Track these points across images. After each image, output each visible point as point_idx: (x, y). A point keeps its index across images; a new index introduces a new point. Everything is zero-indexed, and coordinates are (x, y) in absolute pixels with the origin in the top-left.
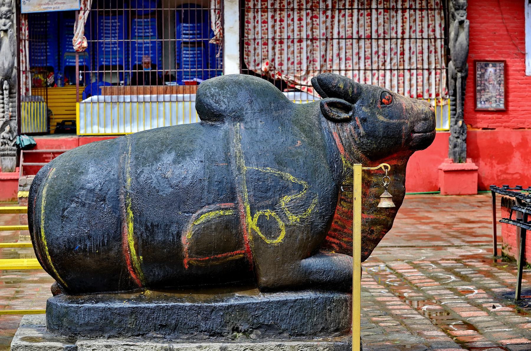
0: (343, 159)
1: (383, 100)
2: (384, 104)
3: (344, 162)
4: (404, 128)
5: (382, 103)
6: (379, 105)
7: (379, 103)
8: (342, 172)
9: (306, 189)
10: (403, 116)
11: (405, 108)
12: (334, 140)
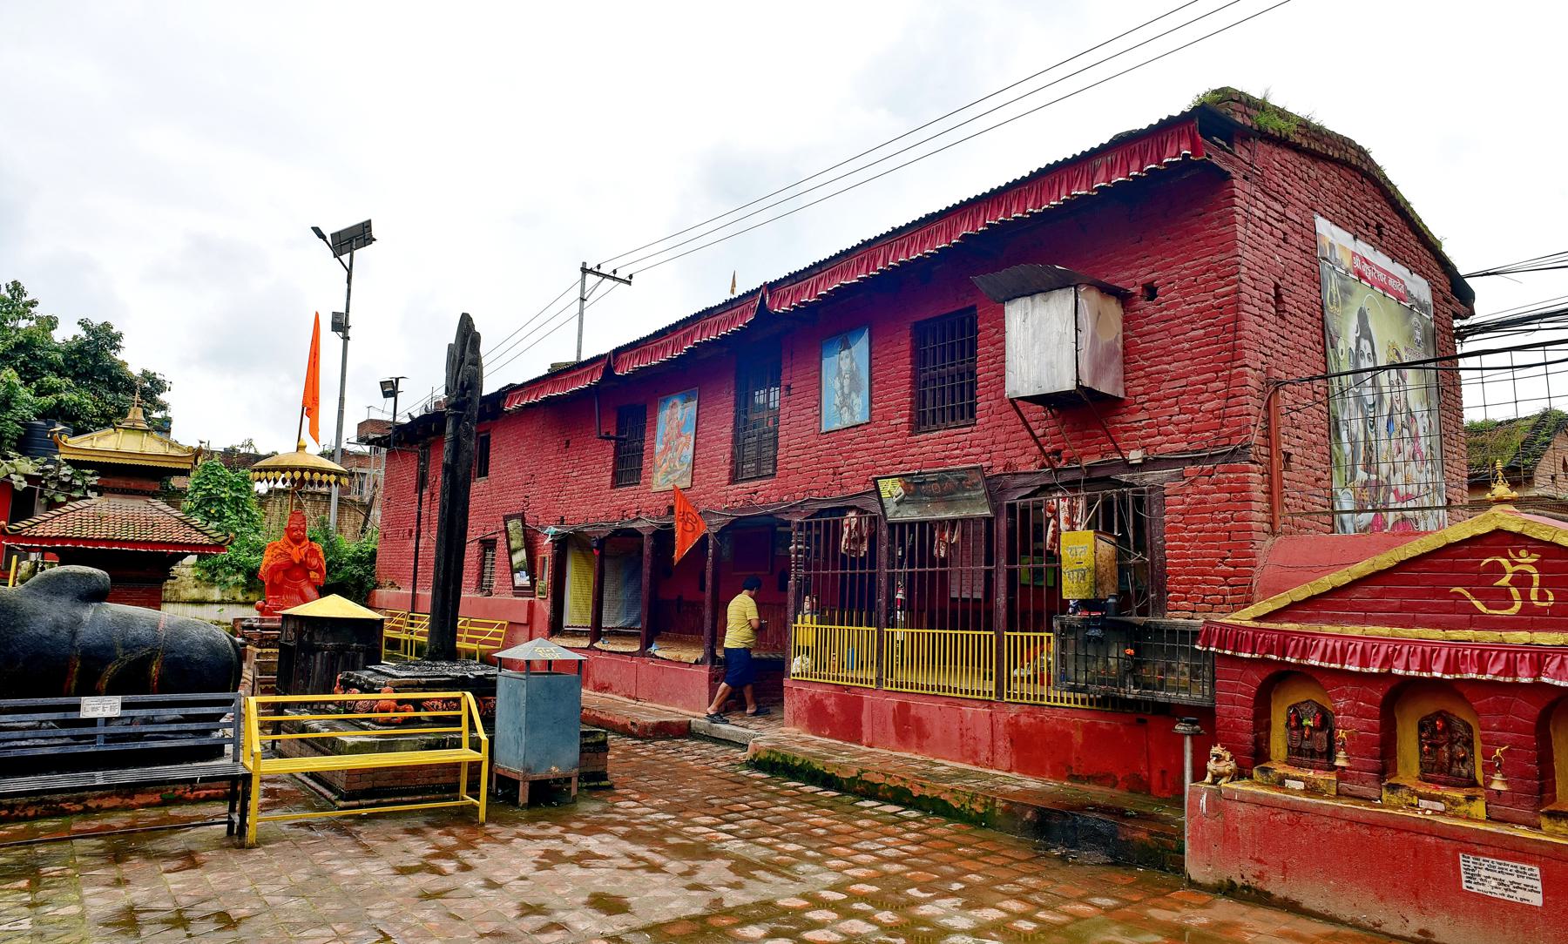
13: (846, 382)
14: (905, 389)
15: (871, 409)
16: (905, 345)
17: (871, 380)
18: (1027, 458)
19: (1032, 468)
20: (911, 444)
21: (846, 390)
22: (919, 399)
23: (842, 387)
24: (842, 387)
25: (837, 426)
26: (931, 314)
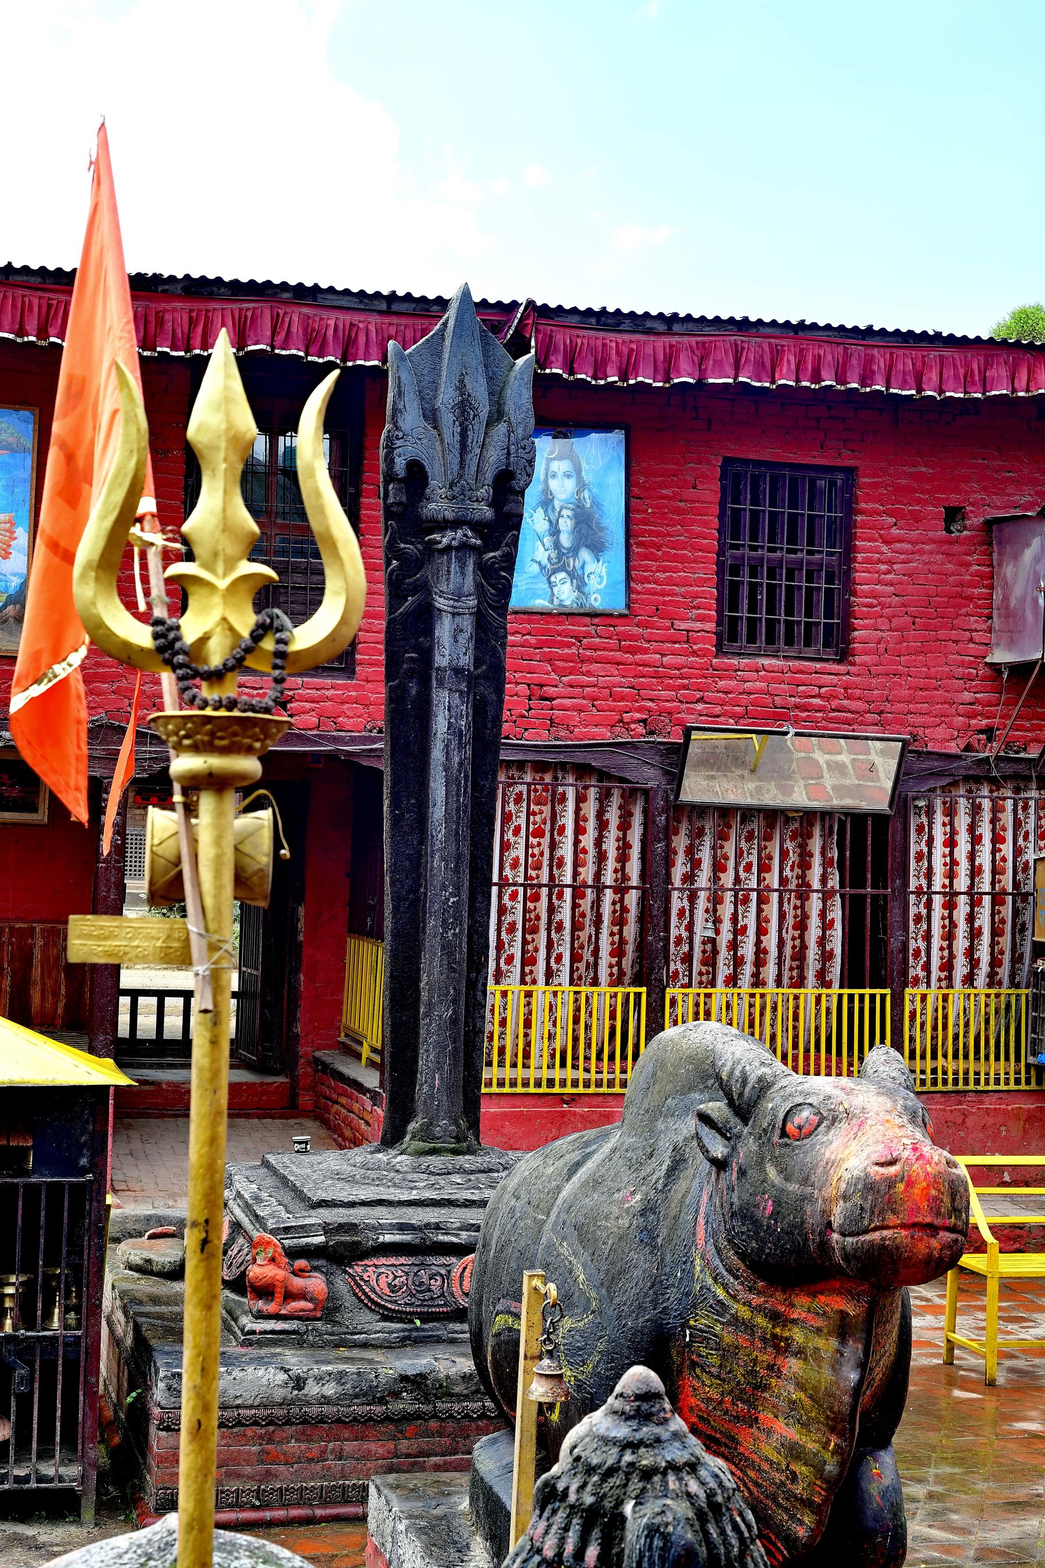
0: (698, 1261)
1: (790, 1127)
2: (788, 1137)
3: (698, 1268)
4: (808, 1209)
5: (784, 1134)
6: (776, 1138)
7: (778, 1132)
8: (688, 1294)
9: (593, 1312)
10: (813, 1178)
11: (827, 1155)
12: (697, 1211)
13: (566, 525)
14: (707, 571)
15: (629, 590)
16: (710, 492)
17: (628, 534)
18: (940, 732)
19: (953, 748)
20: (728, 672)
21: (565, 540)
22: (729, 597)
23: (555, 532)
24: (555, 532)
25: (541, 603)
26: (767, 455)
